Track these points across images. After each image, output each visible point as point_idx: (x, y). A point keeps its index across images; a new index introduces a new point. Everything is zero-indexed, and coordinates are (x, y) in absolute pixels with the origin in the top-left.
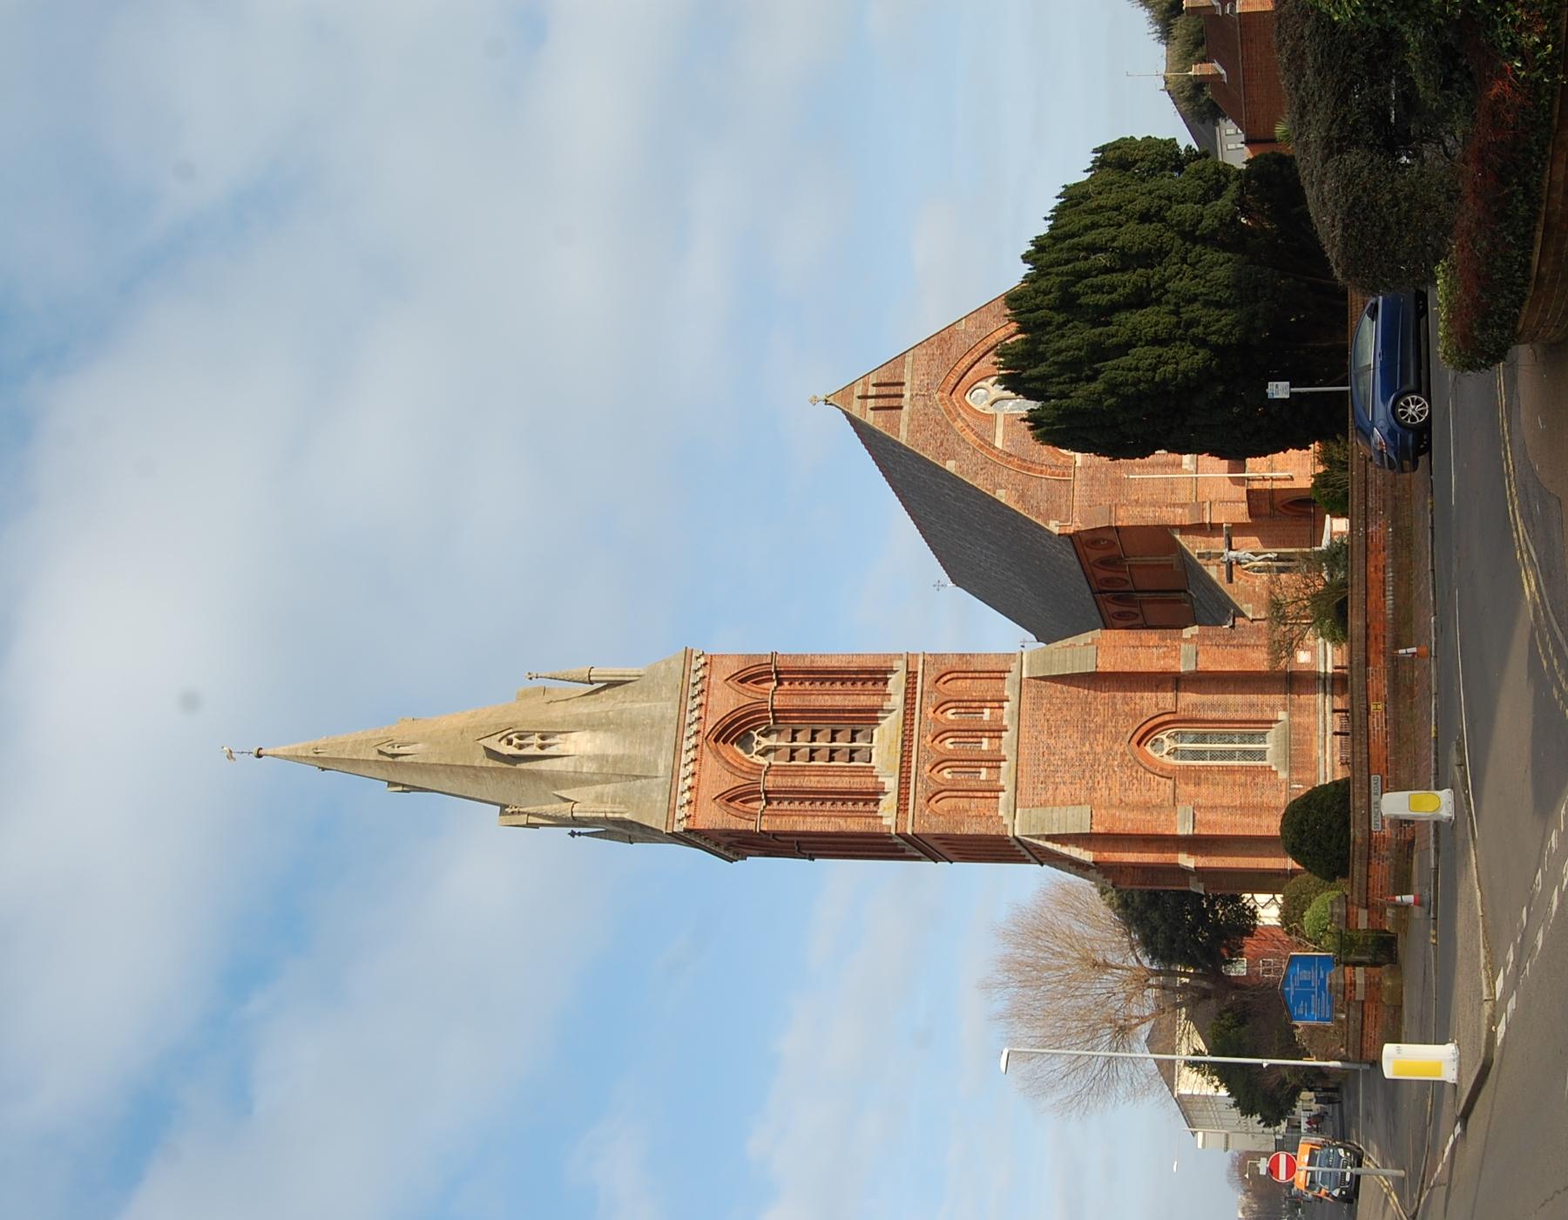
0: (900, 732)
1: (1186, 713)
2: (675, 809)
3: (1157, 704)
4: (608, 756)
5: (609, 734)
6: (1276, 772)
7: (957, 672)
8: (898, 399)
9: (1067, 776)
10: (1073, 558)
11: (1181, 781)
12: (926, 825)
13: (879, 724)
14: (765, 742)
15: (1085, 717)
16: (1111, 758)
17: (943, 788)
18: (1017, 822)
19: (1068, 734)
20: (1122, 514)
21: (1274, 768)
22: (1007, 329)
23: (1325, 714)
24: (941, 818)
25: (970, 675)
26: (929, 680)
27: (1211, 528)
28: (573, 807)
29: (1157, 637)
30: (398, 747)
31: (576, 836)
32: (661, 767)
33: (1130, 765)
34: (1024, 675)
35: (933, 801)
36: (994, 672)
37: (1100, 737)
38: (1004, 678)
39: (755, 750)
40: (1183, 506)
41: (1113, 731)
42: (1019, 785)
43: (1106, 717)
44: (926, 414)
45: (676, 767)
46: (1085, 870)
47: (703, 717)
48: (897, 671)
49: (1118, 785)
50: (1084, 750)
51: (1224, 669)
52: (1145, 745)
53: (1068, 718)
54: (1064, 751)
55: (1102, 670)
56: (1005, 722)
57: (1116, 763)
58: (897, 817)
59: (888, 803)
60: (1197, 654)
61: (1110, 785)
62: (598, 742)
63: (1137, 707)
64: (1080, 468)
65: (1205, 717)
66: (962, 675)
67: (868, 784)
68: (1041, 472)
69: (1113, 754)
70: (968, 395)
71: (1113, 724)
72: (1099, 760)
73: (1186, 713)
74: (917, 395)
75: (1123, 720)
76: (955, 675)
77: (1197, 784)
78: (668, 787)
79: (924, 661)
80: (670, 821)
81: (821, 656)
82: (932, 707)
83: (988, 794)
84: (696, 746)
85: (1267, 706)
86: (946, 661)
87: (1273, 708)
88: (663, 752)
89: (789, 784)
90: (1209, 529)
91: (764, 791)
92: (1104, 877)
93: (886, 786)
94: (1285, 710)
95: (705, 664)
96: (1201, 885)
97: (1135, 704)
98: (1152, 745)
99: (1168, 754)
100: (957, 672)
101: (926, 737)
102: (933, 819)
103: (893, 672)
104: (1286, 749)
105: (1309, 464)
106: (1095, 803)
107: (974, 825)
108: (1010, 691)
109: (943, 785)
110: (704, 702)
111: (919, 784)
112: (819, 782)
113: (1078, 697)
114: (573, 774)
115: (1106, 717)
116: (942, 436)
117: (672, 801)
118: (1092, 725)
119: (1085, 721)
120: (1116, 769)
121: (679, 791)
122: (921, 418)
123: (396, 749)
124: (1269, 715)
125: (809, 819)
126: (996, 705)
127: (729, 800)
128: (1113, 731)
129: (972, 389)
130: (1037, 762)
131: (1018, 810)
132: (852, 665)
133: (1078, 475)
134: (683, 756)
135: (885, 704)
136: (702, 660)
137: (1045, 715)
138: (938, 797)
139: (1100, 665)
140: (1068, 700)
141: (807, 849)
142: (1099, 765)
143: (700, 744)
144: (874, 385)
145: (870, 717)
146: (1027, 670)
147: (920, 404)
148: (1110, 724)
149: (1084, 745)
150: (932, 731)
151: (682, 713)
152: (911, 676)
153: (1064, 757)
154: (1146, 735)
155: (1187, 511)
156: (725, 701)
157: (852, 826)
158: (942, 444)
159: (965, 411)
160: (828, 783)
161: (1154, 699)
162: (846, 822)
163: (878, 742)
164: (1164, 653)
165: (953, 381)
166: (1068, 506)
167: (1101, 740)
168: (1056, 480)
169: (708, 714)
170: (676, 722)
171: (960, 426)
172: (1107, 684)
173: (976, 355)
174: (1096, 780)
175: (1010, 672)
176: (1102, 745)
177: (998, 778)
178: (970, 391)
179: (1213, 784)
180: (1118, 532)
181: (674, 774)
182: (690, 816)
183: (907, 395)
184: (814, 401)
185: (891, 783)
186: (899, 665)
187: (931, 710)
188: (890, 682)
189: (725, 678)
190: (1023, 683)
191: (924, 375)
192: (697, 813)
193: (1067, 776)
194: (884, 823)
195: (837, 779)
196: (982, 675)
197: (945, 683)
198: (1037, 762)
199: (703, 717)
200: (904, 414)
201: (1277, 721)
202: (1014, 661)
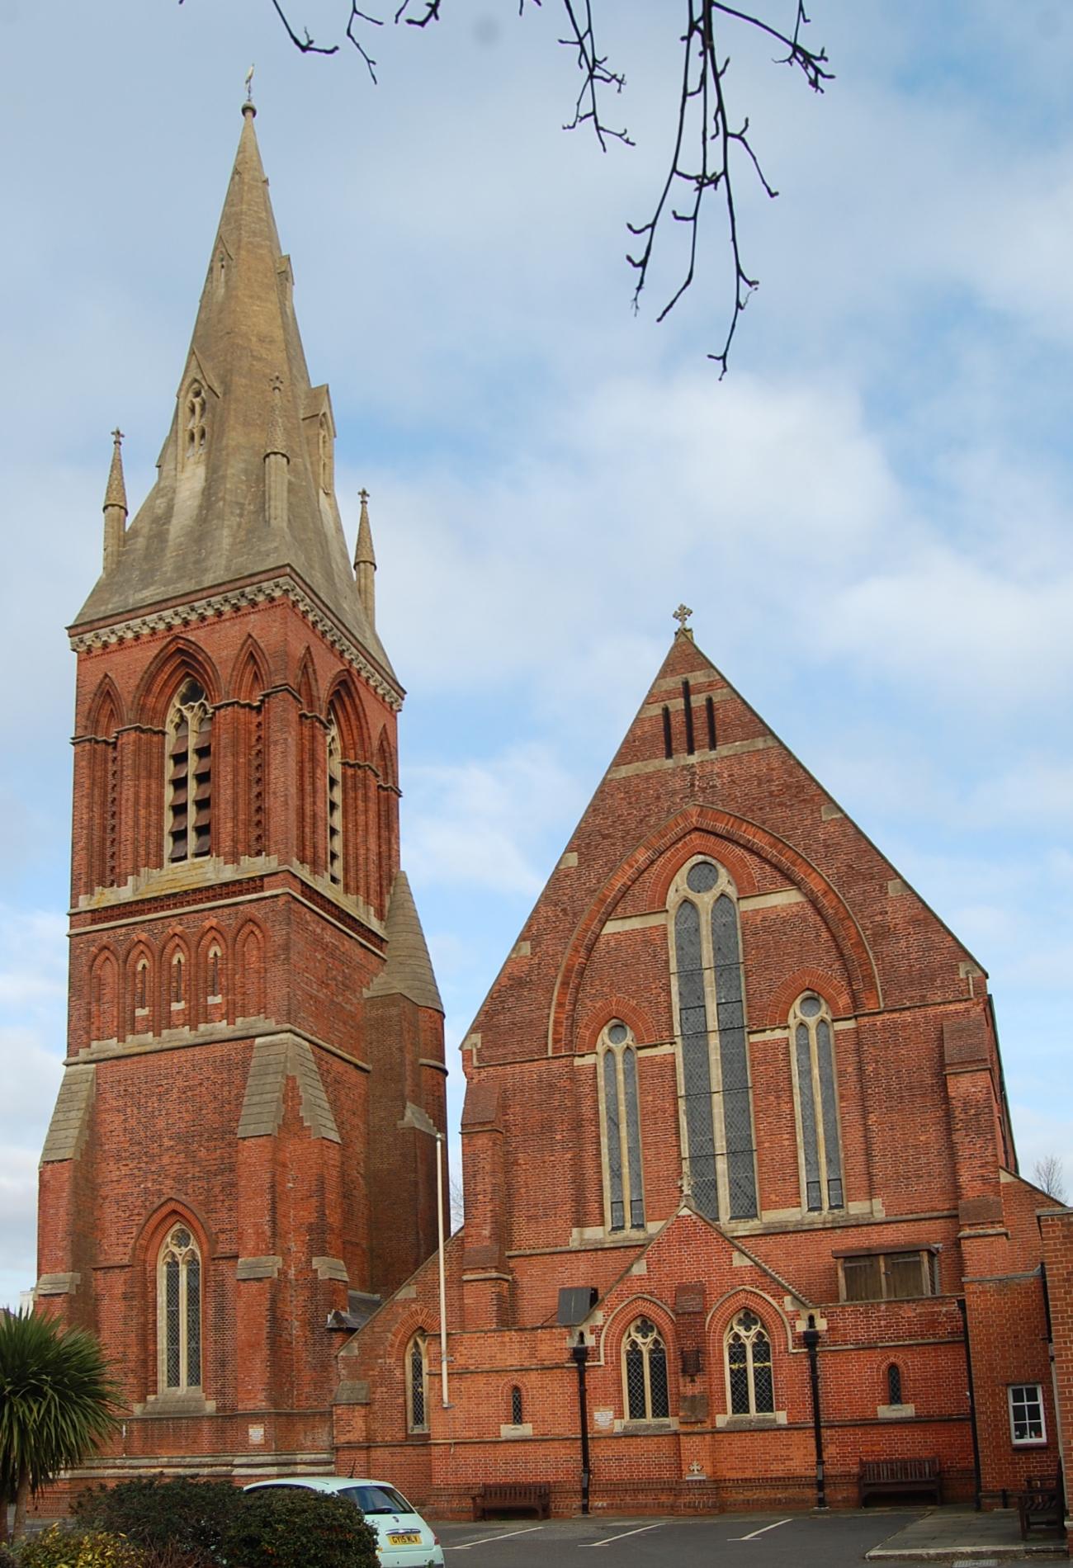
1: (212, 1273)
2: (94, 630)
3: (222, 1231)
6: (142, 1399)
8: (685, 746)
9: (133, 1122)
11: (129, 1275)
15: (206, 1135)
16: (156, 1177)
19: (185, 1115)
20: (480, 1142)
22: (825, 894)
23: (212, 1466)
29: (312, 1220)
33: (147, 1203)
34: (258, 1041)
37: (182, 1158)
41: (189, 1176)
42: (123, 1061)
43: (206, 1163)
44: (658, 798)
50: (165, 1140)
53: (204, 1112)
54: (163, 1113)
57: (149, 1185)
60: (259, 1280)
61: (124, 1181)
63: (220, 1204)
68: (560, 1005)
69: (160, 1179)
70: (700, 858)
71: (197, 1174)
72: (154, 1161)
73: (212, 1273)
77: (125, 1296)
79: (276, 896)
82: (218, 923)
85: (223, 1386)
86: (278, 928)
94: (218, 1409)
98: (182, 1231)
101: (181, 924)
104: (169, 1413)
105: (468, 1434)
106: (103, 1165)
115: (206, 1163)
116: (620, 834)
120: (142, 1186)
122: (651, 792)
128: (189, 1176)
129: (714, 862)
131: (94, 1066)
142: (147, 1163)
147: (677, 783)
148: (198, 1169)
149: (171, 1139)
158: (605, 837)
159: (669, 860)
160: (127, 813)
161: (228, 1227)
164: (263, 1233)
165: (720, 827)
166: (505, 1056)
167: (177, 1161)
171: (638, 856)
173: (771, 852)
174: (128, 1162)
178: (709, 859)
179: (125, 1317)
187: (214, 922)
190: (248, 1041)
193: (133, 1122)
197: (252, 932)
202: (278, 1023)
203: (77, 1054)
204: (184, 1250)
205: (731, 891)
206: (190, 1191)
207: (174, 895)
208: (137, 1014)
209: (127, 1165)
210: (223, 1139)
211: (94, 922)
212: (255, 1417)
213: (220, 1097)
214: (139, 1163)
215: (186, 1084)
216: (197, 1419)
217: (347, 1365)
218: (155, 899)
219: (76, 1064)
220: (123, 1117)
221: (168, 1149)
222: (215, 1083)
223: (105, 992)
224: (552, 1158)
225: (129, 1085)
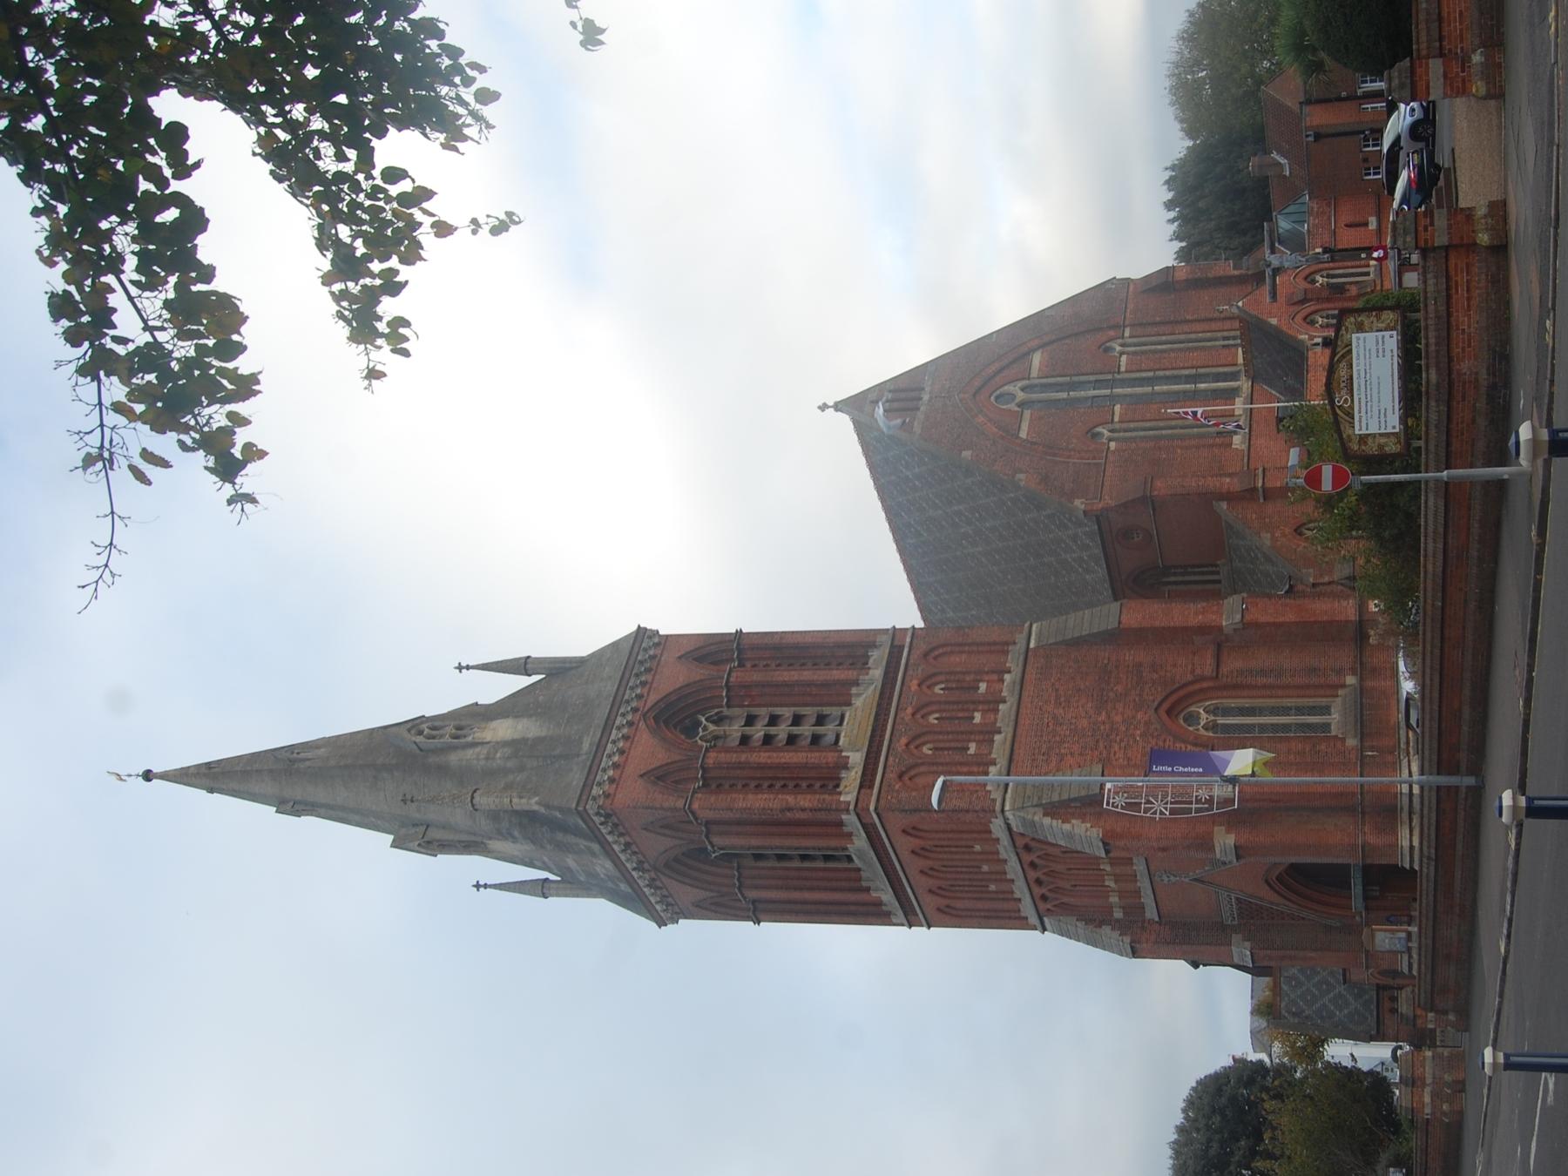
0: (875, 704)
1: (1229, 680)
3: (1193, 671)
4: (528, 739)
5: (534, 719)
6: (1343, 740)
7: (951, 645)
10: (1101, 572)
12: (894, 800)
13: (849, 704)
14: (712, 727)
17: (920, 761)
18: (1009, 795)
20: (1159, 484)
21: (1340, 736)
24: (914, 794)
25: (966, 648)
27: (1265, 499)
28: (472, 798)
30: (298, 753)
31: (482, 889)
32: (586, 746)
33: (1156, 734)
34: (1032, 645)
35: (906, 778)
36: (995, 643)
38: (1008, 652)
39: (701, 734)
40: (1231, 475)
42: (1015, 757)
43: (1129, 686)
45: (604, 742)
46: (1096, 927)
47: (645, 694)
48: (881, 645)
49: (1139, 756)
51: (1277, 620)
52: (1177, 716)
53: (1082, 687)
54: (1074, 721)
55: (1126, 626)
56: (1004, 694)
57: (1138, 732)
58: (859, 793)
59: (852, 779)
61: (1129, 755)
62: (520, 727)
64: (1114, 452)
65: (1254, 683)
66: (957, 649)
67: (831, 757)
68: (1069, 457)
70: (992, 398)
71: (1138, 692)
73: (1229, 680)
74: (936, 397)
75: (1150, 688)
76: (949, 649)
78: (589, 763)
80: (584, 797)
83: (975, 769)
84: (630, 724)
87: (1340, 672)
88: (592, 730)
89: (733, 760)
90: (1262, 500)
91: (702, 767)
92: (1120, 935)
93: (850, 761)
94: (1354, 674)
95: (657, 645)
96: (1248, 944)
97: (1166, 671)
98: (1185, 720)
99: (1206, 728)
100: (951, 645)
102: (903, 795)
103: (873, 645)
107: (954, 801)
108: (1014, 662)
109: (921, 758)
110: (650, 680)
111: (891, 759)
112: (769, 757)
114: (482, 763)
115: (1129, 686)
117: (592, 777)
118: (1112, 695)
120: (1138, 738)
121: (601, 767)
123: (295, 755)
124: (1334, 679)
125: (750, 796)
126: (995, 677)
127: (658, 778)
128: (1137, 699)
129: (998, 392)
130: (1039, 734)
132: (828, 640)
133: (1111, 458)
134: (614, 732)
135: (861, 677)
136: (656, 640)
137: (1053, 684)
138: (913, 773)
139: (1124, 621)
141: (756, 887)
142: (1117, 735)
143: (636, 722)
144: (890, 391)
145: (841, 695)
146: (1035, 640)
150: (914, 703)
151: (622, 689)
152: (895, 651)
153: (1073, 727)
154: (1176, 705)
155: (1236, 480)
156: (673, 677)
157: (802, 803)
162: (796, 798)
163: (848, 724)
165: (977, 383)
167: (1121, 710)
168: (1085, 464)
169: (651, 693)
170: (611, 699)
171: (980, 421)
172: (1132, 652)
175: (1015, 643)
177: (990, 753)
178: (995, 394)
180: (1154, 510)
181: (600, 747)
182: (609, 795)
183: (926, 397)
184: (823, 407)
185: (856, 758)
186: (886, 639)
187: (915, 682)
188: (871, 661)
189: (679, 654)
190: (1030, 654)
191: (946, 380)
192: (618, 792)
194: (842, 799)
195: (791, 754)
196: (980, 649)
197: (935, 658)
198: (1039, 734)
199: (645, 694)
200: (920, 415)
201: (1343, 686)
204: (1204, 715)
205: (1020, 384)
206: (1151, 698)
207: (877, 714)
208: (973, 753)
209: (1115, 753)
211: (871, 787)
212: (1362, 608)
214: (1116, 741)
215: (1053, 702)
216: (1362, 690)
217: (1321, 576)
218: (873, 731)
220: (1069, 756)
221: (1109, 717)
222: (1059, 679)
224: (1179, 459)
225: (1040, 751)
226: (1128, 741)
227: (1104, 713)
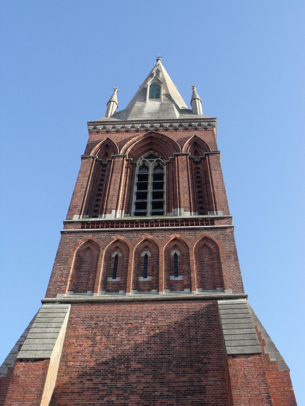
15: (174, 362)
16: (121, 392)
19: (153, 345)
26: (207, 233)
34: (219, 302)
37: (149, 378)
43: (175, 385)
57: (114, 398)
61: (85, 393)
69: (125, 394)
71: (165, 393)
72: (120, 378)
79: (225, 228)
81: (221, 174)
113: (198, 353)
115: (175, 385)
118: (164, 370)
119: (169, 362)
120: (106, 399)
128: (156, 393)
140: (194, 344)
142: (112, 380)
149: (139, 362)
167: (143, 380)
172: (218, 383)
176: (139, 382)
202: (234, 292)
203: (55, 296)
210: (191, 366)
213: (187, 335)
219: (53, 302)
221: (135, 371)
223: (83, 265)
226: (103, 390)
227: (139, 366)
